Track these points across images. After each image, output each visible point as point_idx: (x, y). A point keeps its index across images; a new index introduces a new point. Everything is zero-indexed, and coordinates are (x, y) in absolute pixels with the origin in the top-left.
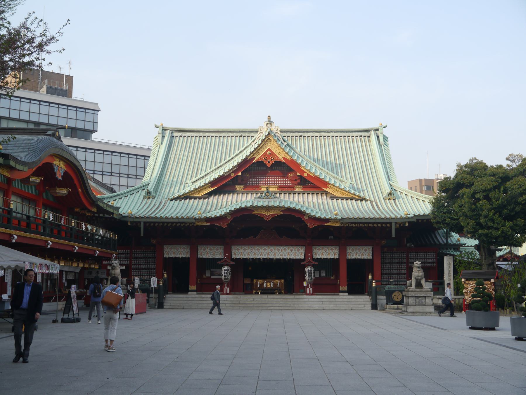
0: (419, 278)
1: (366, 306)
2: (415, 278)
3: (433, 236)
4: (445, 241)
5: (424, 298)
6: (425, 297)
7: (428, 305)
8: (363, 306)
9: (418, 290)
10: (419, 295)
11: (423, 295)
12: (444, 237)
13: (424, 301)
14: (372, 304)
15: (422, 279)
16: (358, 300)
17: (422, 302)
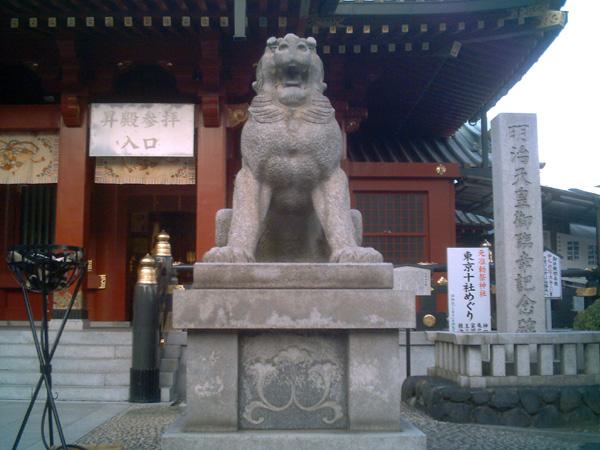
0: (294, 164)
1: (111, 379)
2: (263, 175)
3: (442, 148)
4: (480, 160)
5: (327, 349)
6: (340, 337)
7: (366, 425)
8: (95, 380)
9: (270, 270)
10: (275, 322)
11: (317, 321)
12: (474, 151)
13: (325, 375)
14: (135, 375)
15: (324, 176)
16: (92, 352)
17: (311, 394)
